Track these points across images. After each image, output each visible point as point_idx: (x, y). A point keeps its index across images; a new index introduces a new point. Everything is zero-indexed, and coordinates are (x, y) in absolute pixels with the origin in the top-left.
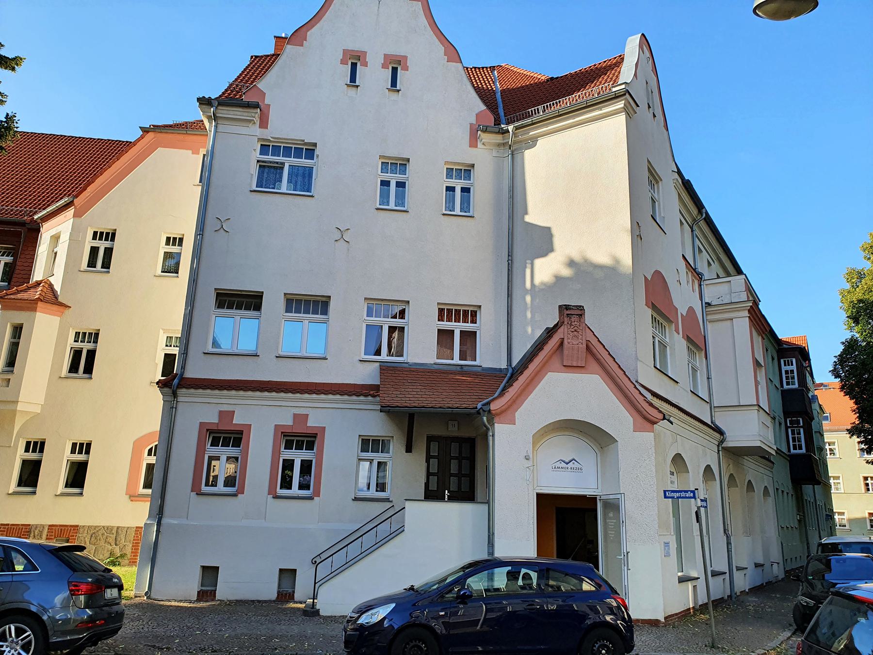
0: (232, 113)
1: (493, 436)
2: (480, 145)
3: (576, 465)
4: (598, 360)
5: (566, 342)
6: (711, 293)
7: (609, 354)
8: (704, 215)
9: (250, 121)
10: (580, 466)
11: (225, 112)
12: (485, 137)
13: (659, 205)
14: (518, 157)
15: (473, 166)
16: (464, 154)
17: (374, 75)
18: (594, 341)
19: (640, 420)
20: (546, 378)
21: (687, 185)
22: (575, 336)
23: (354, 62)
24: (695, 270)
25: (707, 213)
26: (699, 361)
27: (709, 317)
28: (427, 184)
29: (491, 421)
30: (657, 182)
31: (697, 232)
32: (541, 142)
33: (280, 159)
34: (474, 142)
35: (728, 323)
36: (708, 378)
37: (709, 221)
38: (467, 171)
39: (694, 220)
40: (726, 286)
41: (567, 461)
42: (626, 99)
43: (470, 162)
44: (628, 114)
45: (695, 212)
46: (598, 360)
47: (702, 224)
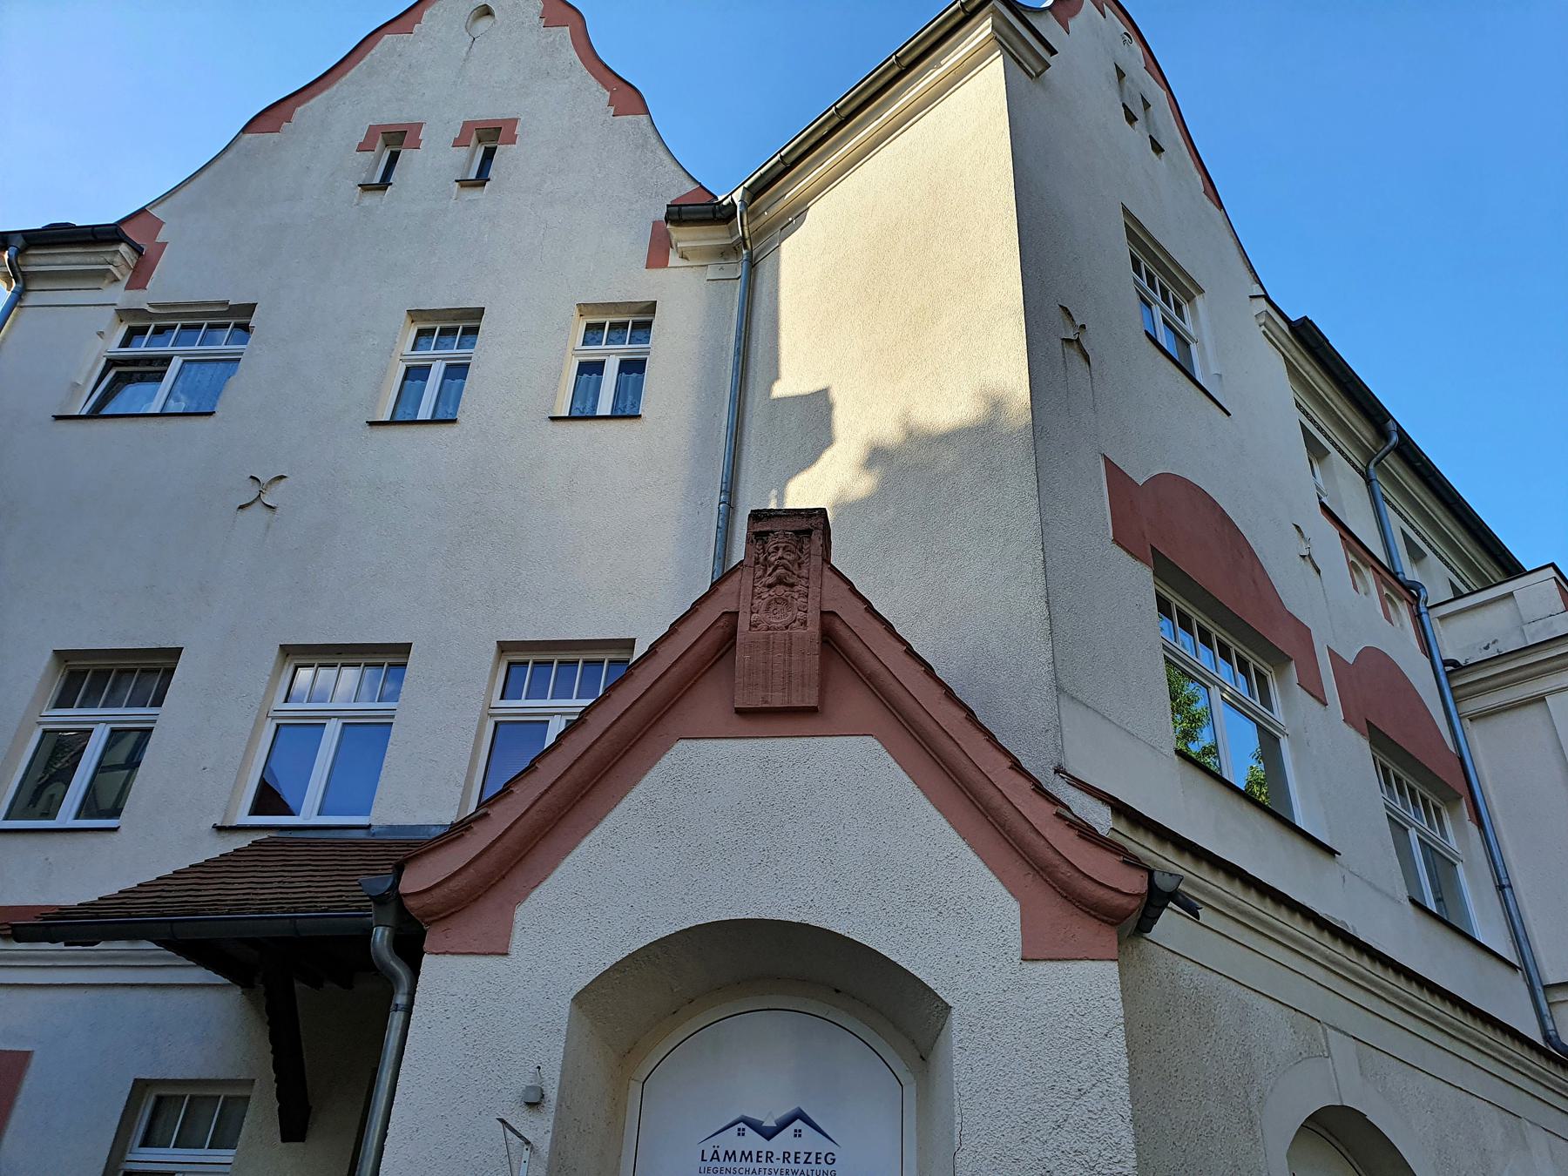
0: (59, 260)
1: (408, 1010)
2: (674, 259)
3: (810, 1141)
4: (869, 681)
5: (743, 623)
6: (1456, 641)
7: (910, 651)
8: (1395, 438)
9: (103, 274)
10: (824, 1146)
11: (43, 260)
12: (684, 237)
13: (1202, 350)
14: (764, 268)
15: (651, 307)
16: (638, 284)
17: (435, 161)
18: (850, 613)
19: (1052, 908)
20: (666, 761)
21: (1306, 336)
22: (777, 600)
23: (395, 140)
24: (1394, 576)
25: (1401, 432)
26: (1459, 837)
27: (1472, 706)
28: (529, 355)
29: (411, 951)
30: (1190, 299)
31: (1383, 487)
32: (815, 211)
33: (168, 349)
34: (658, 254)
35: (1533, 712)
36: (1500, 888)
37: (1409, 453)
38: (640, 320)
39: (1369, 456)
40: (1503, 609)
41: (770, 1123)
42: (995, 11)
43: (644, 297)
44: (1014, 60)
45: (1366, 433)
46: (869, 681)
47: (1393, 463)
